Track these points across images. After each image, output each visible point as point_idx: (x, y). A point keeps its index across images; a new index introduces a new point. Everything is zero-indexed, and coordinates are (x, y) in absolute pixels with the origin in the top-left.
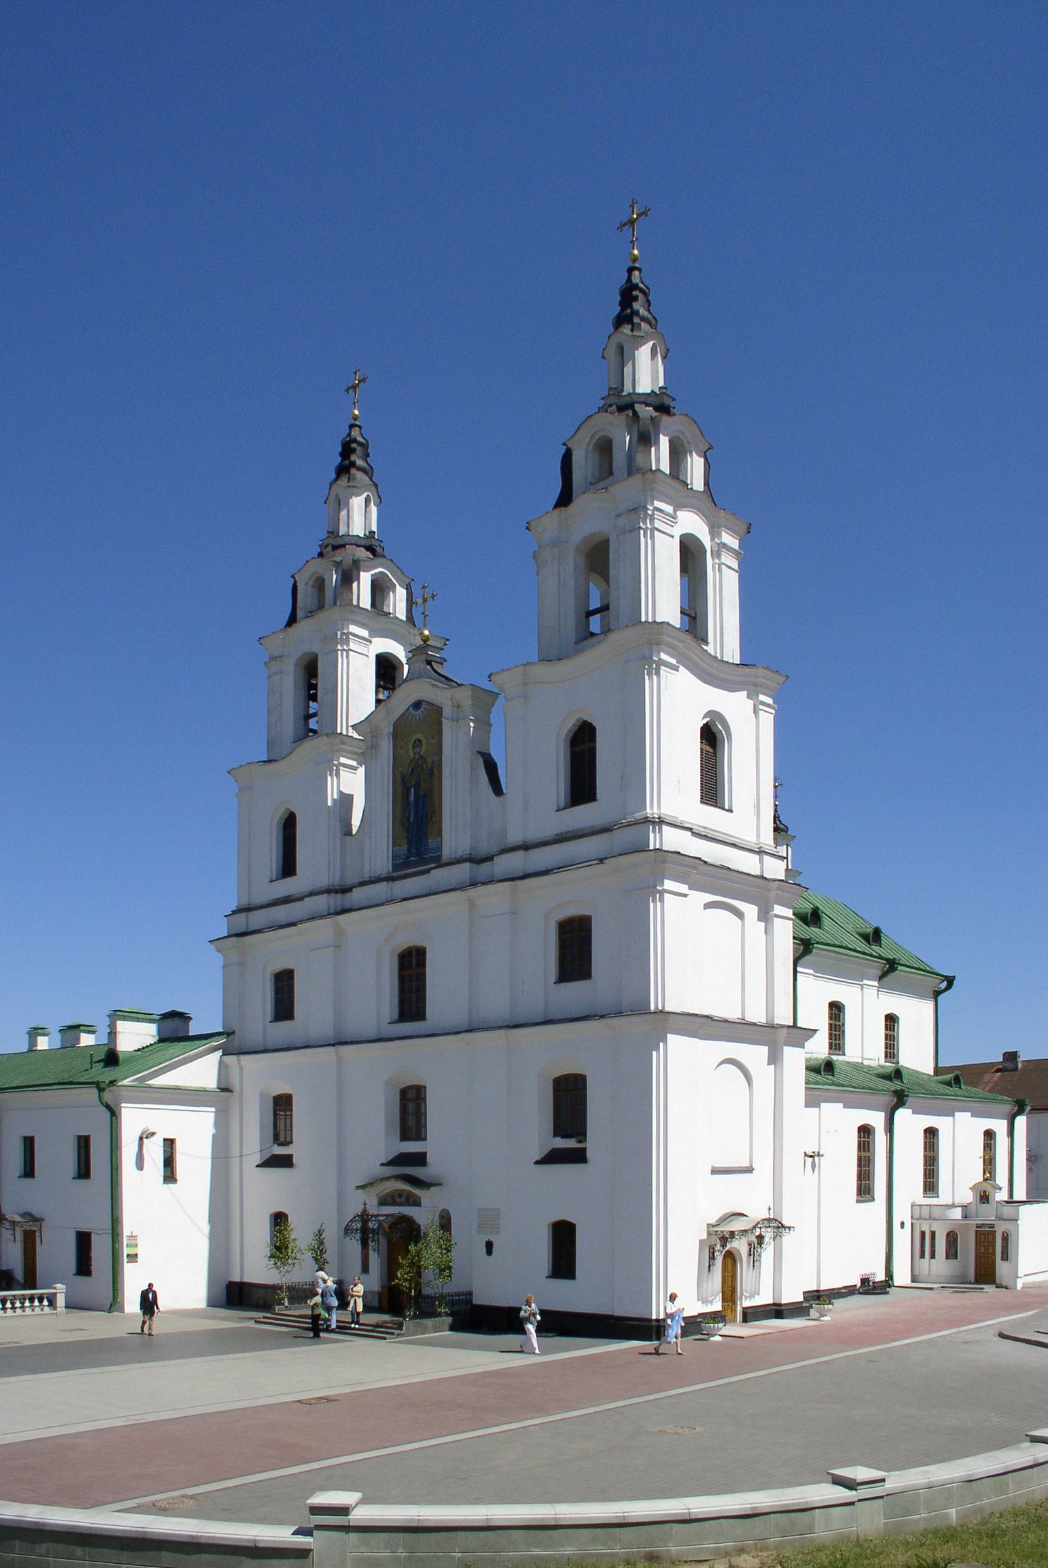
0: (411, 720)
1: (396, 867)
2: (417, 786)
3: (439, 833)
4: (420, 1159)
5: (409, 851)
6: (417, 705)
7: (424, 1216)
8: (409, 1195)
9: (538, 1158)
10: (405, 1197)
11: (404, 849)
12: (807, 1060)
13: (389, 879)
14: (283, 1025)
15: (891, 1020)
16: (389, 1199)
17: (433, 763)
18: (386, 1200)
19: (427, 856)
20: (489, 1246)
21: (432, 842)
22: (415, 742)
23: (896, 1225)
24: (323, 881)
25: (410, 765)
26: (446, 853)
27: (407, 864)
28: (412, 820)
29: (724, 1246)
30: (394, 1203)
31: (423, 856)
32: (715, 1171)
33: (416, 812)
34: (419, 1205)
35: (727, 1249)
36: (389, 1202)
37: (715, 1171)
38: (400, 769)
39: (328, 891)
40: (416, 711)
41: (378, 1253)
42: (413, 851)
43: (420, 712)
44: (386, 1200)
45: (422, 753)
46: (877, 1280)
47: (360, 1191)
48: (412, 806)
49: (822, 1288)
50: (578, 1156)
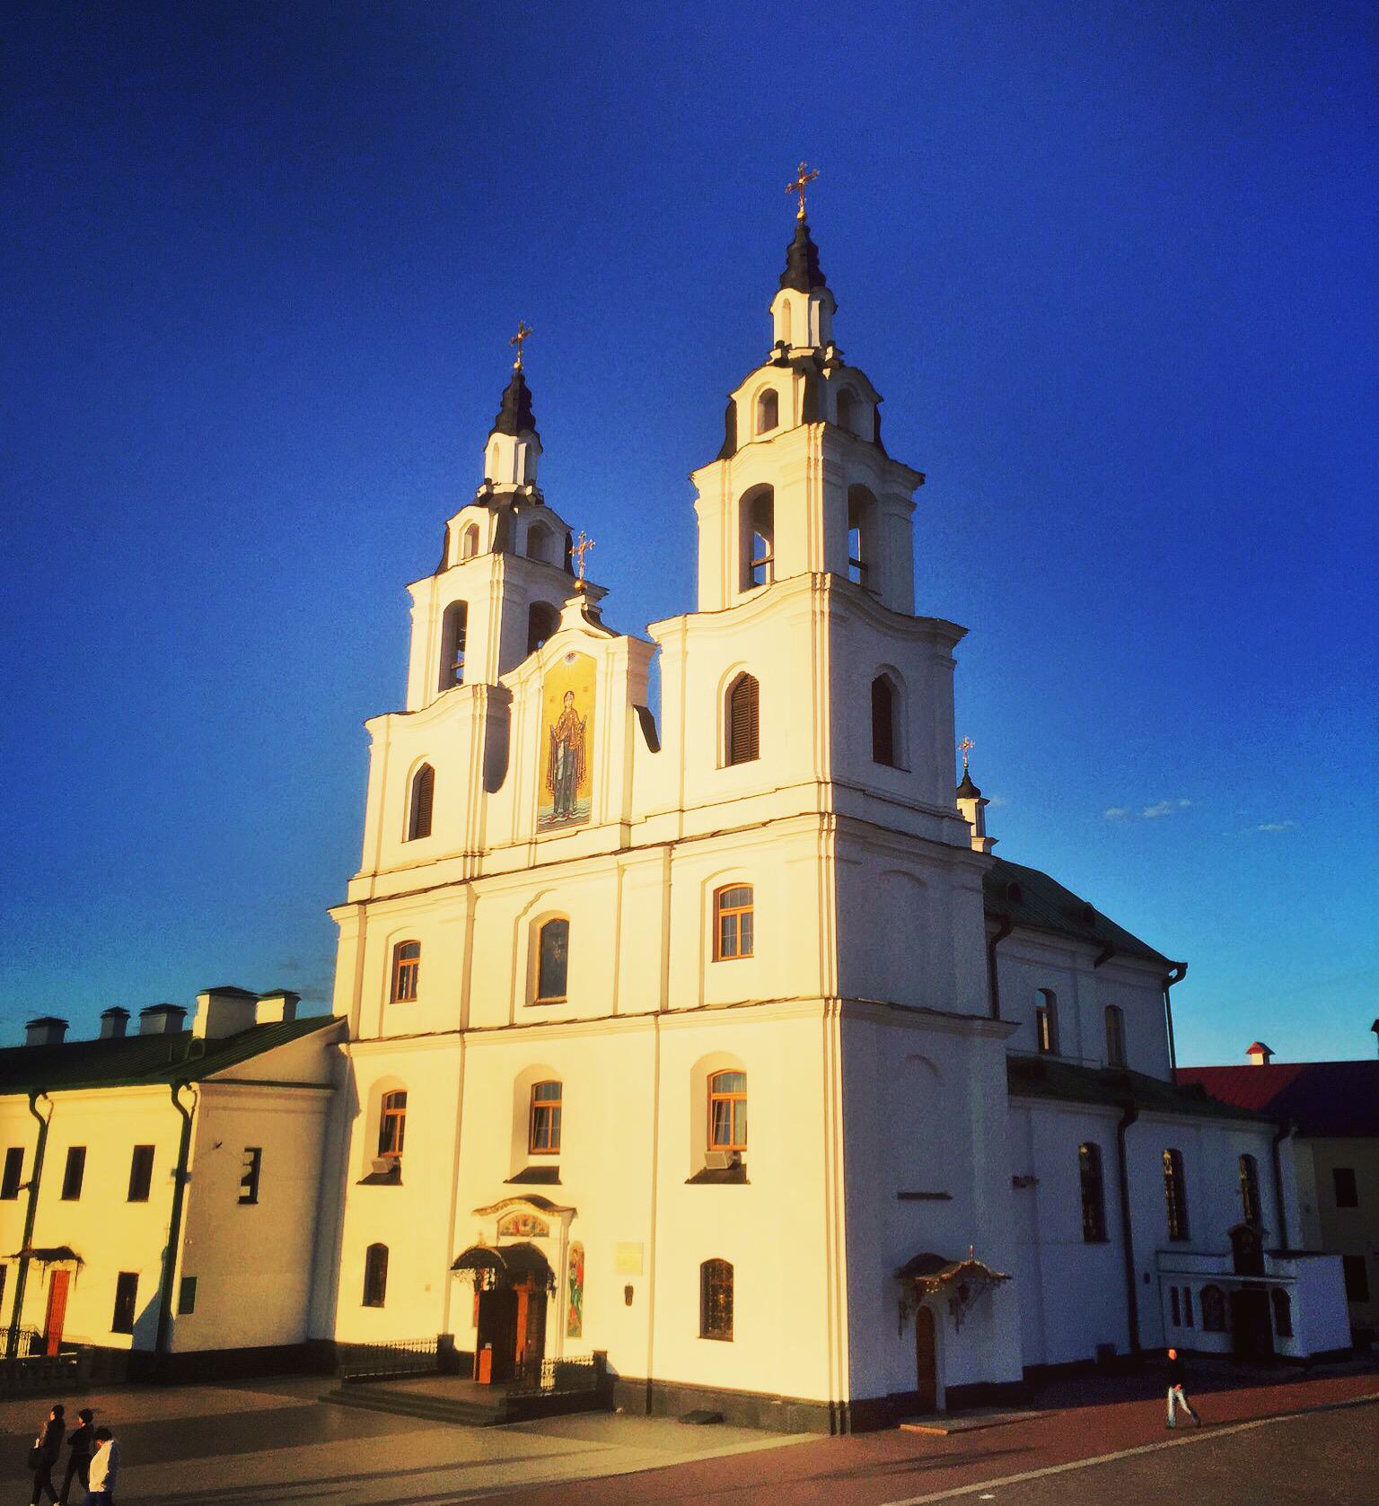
1: (541, 828)
3: (589, 794)
4: (549, 1176)
5: (556, 811)
6: (571, 656)
9: (689, 1176)
10: (531, 1225)
11: (550, 809)
14: (402, 1007)
15: (1113, 1012)
16: (511, 1227)
17: (585, 716)
18: (507, 1228)
20: (629, 1292)
21: (581, 801)
25: (560, 718)
28: (560, 778)
29: (918, 1300)
30: (517, 1232)
31: (570, 816)
32: (903, 1196)
35: (922, 1304)
36: (511, 1231)
37: (903, 1196)
38: (550, 723)
44: (507, 1228)
46: (1120, 1352)
48: (561, 762)
49: (1051, 1361)
50: (735, 1173)
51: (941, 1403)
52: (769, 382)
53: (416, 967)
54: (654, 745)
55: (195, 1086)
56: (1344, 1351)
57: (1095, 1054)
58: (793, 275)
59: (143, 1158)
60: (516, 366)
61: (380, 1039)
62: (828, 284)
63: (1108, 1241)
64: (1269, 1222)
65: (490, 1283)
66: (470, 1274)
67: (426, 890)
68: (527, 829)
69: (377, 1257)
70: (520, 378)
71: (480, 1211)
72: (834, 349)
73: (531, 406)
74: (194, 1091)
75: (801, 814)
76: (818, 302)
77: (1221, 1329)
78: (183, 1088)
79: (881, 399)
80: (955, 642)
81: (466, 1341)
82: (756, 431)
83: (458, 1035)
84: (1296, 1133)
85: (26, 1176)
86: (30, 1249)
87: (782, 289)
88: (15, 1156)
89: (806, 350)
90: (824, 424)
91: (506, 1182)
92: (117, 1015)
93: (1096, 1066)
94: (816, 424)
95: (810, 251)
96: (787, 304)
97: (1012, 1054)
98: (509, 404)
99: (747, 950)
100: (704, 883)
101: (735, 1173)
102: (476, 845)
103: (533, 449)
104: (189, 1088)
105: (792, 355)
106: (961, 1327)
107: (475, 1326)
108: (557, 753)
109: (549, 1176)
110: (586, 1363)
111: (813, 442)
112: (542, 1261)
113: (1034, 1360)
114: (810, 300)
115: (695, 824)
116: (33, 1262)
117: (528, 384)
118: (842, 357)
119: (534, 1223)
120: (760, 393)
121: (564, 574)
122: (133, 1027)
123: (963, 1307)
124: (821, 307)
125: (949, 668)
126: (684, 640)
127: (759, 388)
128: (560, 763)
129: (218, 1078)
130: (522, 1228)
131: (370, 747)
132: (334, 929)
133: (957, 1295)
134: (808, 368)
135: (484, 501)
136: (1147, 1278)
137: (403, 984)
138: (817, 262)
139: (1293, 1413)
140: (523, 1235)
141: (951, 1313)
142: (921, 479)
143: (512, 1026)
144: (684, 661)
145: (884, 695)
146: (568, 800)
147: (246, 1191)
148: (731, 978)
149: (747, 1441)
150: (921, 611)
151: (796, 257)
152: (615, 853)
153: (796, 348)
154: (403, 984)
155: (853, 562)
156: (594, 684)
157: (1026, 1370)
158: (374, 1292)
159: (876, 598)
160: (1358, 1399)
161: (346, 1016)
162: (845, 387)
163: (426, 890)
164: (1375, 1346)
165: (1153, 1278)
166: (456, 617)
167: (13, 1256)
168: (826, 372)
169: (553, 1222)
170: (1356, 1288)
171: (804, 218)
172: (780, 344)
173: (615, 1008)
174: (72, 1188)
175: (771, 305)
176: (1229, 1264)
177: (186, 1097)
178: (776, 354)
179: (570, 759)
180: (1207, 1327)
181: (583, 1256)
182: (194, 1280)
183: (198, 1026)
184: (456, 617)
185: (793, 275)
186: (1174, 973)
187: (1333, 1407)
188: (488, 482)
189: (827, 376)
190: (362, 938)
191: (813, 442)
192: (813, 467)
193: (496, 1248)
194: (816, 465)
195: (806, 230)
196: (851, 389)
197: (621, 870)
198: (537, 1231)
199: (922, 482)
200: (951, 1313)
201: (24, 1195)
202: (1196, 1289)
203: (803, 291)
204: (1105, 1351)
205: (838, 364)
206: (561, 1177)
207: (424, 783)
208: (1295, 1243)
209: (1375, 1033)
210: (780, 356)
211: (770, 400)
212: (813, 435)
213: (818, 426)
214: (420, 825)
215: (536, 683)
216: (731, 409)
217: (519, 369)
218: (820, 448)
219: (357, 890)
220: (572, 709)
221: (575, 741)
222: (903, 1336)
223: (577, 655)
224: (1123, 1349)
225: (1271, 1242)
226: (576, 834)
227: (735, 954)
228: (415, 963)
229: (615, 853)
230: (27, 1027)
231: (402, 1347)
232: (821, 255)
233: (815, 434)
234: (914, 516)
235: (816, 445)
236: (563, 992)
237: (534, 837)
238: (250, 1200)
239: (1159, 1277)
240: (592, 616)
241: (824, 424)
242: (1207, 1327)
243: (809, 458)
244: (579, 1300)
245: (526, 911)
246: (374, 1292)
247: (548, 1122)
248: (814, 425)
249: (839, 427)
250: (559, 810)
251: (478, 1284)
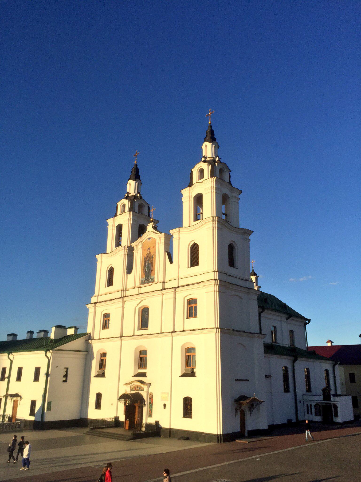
1: (142, 284)
3: (154, 274)
4: (144, 375)
5: (145, 279)
6: (149, 238)
8: (140, 387)
9: (180, 375)
10: (139, 388)
12: (264, 344)
15: (292, 332)
16: (134, 388)
17: (153, 254)
20: (165, 405)
21: (152, 276)
23: (298, 402)
26: (156, 280)
28: (146, 270)
30: (135, 390)
32: (236, 380)
34: (143, 390)
35: (241, 408)
36: (134, 389)
37: (236, 380)
38: (144, 256)
46: (293, 421)
48: (147, 266)
49: (275, 423)
50: (192, 374)
51: (246, 434)
52: (201, 167)
53: (109, 320)
54: (171, 262)
55: (51, 351)
56: (352, 421)
57: (287, 343)
58: (208, 138)
59: (37, 370)
60: (135, 162)
61: (99, 339)
62: (217, 141)
63: (290, 392)
64: (332, 387)
65: (128, 403)
66: (123, 401)
67: (112, 300)
68: (138, 284)
69: (99, 396)
70: (136, 165)
71: (126, 384)
72: (218, 158)
73: (139, 173)
74: (51, 353)
75: (210, 280)
76: (214, 145)
77: (320, 415)
78: (48, 352)
79: (231, 171)
80: (250, 235)
81: (122, 418)
82: (198, 180)
83: (120, 338)
84: (339, 364)
85: (7, 375)
86: (8, 394)
87: (205, 142)
88: (4, 370)
89: (211, 158)
90: (216, 178)
91: (132, 376)
92: (31, 333)
93: (287, 346)
94: (214, 177)
95: (212, 132)
96: (206, 146)
97: (265, 343)
98: (133, 172)
99: (196, 315)
100: (184, 298)
101: (192, 374)
102: (125, 288)
103: (140, 184)
104: (50, 352)
105: (208, 159)
106: (251, 414)
107: (124, 414)
108: (146, 264)
109: (144, 375)
110: (153, 424)
111: (213, 182)
112: (142, 397)
113: (271, 423)
114: (212, 145)
115: (182, 283)
116: (9, 398)
117: (138, 167)
118: (220, 160)
119: (140, 387)
120: (199, 169)
121: (148, 217)
122: (35, 336)
123: (252, 409)
124: (215, 147)
125: (248, 241)
126: (179, 234)
127: (199, 168)
128: (147, 266)
129: (57, 349)
130: (137, 389)
131: (97, 262)
132: (87, 310)
133: (251, 406)
134: (212, 163)
135: (127, 198)
136: (300, 402)
137: (106, 325)
138: (214, 135)
139: (338, 437)
140: (137, 390)
142: (241, 192)
143: (134, 335)
144: (179, 240)
145: (231, 248)
146: (149, 276)
147: (64, 379)
148: (192, 323)
149: (196, 444)
150: (241, 227)
151: (209, 134)
152: (161, 290)
153: (209, 158)
154: (106, 325)
155: (223, 214)
156: (155, 246)
157: (269, 426)
158: (98, 406)
159: (229, 223)
160: (355, 434)
161: (91, 333)
162: (221, 168)
163: (112, 300)
164: (360, 419)
165: (302, 402)
166: (120, 228)
167: (3, 396)
168: (216, 164)
169: (145, 387)
170: (355, 404)
171: (210, 123)
172: (204, 157)
173: (161, 331)
174: (19, 378)
175: (202, 146)
176: (322, 398)
177: (49, 354)
178: (203, 159)
179: (149, 265)
180: (316, 415)
181: (153, 396)
182: (51, 402)
183: (52, 336)
184: (120, 228)
185: (208, 138)
186: (307, 322)
187: (349, 436)
188: (128, 193)
189: (217, 165)
190: (95, 312)
191: (213, 182)
192: (213, 189)
193: (130, 394)
194: (214, 188)
195: (211, 126)
196: (223, 168)
197: (163, 295)
198: (141, 389)
199: (241, 193)
200: (249, 411)
201: (6, 380)
202: (313, 404)
203: (210, 142)
204: (289, 421)
205: (220, 162)
206: (147, 375)
207: (111, 272)
208: (339, 393)
209: (360, 337)
210: (204, 160)
211: (201, 171)
212: (213, 180)
213: (214, 178)
214: (110, 283)
215: (140, 246)
216: (191, 174)
217: (136, 163)
218: (215, 184)
219: (94, 300)
220: (150, 252)
221: (150, 261)
222: (236, 417)
223: (151, 238)
224: (294, 420)
225: (333, 392)
226: (151, 285)
227: (193, 317)
228: (109, 319)
229: (161, 290)
231: (105, 420)
232: (215, 133)
233: (214, 180)
234: (239, 202)
235: (214, 183)
236: (148, 327)
237: (140, 286)
238: (65, 381)
239: (303, 401)
240: (155, 228)
241: (216, 178)
242: (316, 415)
243: (212, 186)
244: (152, 407)
245: (138, 305)
246: (98, 406)
247: (143, 361)
248: (213, 178)
249: (220, 178)
250: (146, 279)
251: (125, 403)
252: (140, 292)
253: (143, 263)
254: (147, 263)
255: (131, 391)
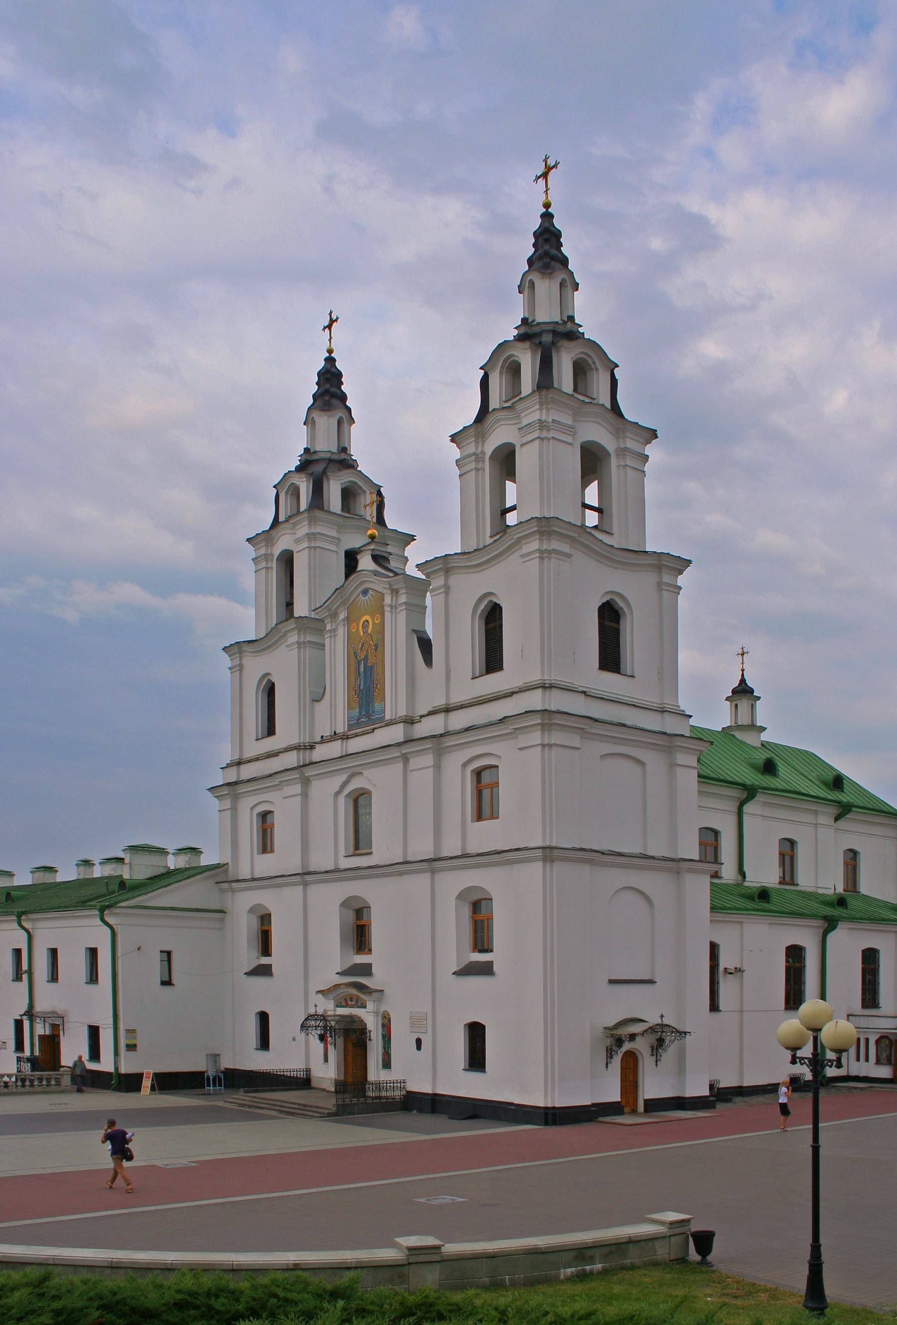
0: (361, 604)
1: (351, 727)
2: (366, 659)
3: (383, 699)
4: (366, 969)
5: (360, 713)
7: (369, 1017)
8: (358, 999)
9: (455, 969)
11: (356, 713)
13: (345, 737)
19: (373, 718)
20: (419, 1042)
21: (377, 706)
22: (364, 622)
24: (295, 741)
27: (358, 724)
28: (362, 688)
30: (347, 1006)
33: (365, 682)
34: (365, 1007)
39: (297, 748)
40: (364, 597)
41: (335, 1047)
42: (363, 713)
43: (367, 597)
45: (369, 631)
47: (320, 995)
75: (526, 712)
92: (87, 863)
122: (98, 872)
128: (361, 677)
130: (350, 1003)
141: (652, 1055)
149: (489, 1128)
161: (228, 864)
198: (359, 1004)
221: (371, 660)
223: (370, 592)
226: (373, 731)
230: (31, 872)
244: (389, 1047)
250: (363, 713)
252: (346, 752)
253: (353, 669)
254: (362, 666)
255: (338, 1009)
